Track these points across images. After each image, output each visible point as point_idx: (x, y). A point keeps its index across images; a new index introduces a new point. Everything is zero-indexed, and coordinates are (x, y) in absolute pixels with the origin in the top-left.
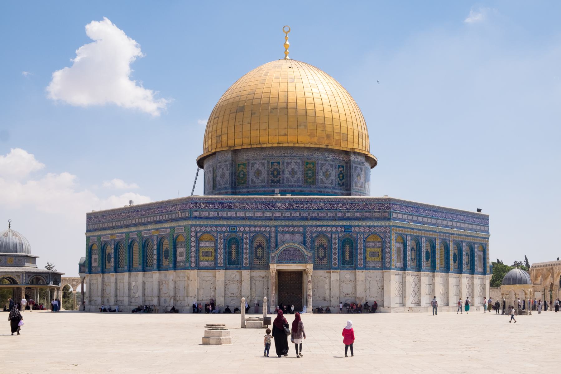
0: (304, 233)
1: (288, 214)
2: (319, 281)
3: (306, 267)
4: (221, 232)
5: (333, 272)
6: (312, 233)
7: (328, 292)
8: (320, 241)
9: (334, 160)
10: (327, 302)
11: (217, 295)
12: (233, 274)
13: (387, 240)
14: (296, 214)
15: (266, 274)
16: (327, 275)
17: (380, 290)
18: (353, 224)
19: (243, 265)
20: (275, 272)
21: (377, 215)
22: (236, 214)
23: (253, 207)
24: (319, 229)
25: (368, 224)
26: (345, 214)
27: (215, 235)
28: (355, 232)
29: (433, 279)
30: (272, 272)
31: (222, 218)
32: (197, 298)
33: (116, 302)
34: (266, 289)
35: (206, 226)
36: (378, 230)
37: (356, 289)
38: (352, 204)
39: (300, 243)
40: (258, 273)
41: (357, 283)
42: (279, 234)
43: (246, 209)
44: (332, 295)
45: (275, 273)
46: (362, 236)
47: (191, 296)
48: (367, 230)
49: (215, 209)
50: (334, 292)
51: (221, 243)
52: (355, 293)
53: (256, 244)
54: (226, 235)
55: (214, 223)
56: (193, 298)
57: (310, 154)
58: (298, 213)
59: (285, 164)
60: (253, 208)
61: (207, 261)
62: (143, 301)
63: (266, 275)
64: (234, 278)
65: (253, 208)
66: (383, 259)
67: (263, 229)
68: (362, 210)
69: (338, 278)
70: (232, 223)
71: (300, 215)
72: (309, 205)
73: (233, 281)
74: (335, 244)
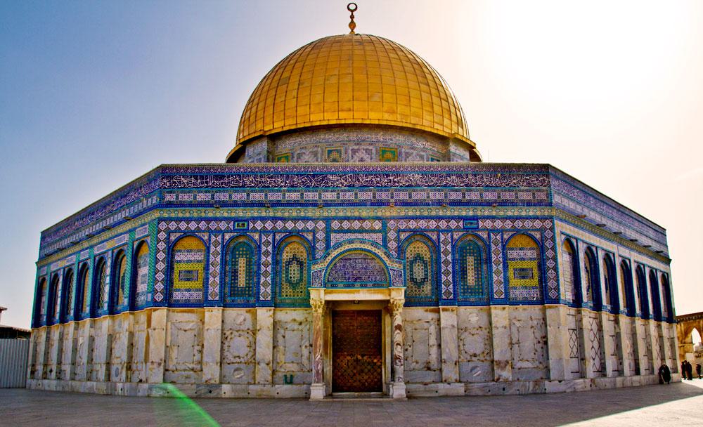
0: (384, 230)
1: (350, 196)
2: (416, 329)
3: (390, 295)
4: (218, 231)
5: (444, 310)
6: (399, 231)
7: (434, 350)
8: (415, 248)
9: (424, 150)
10: (433, 372)
11: (205, 359)
12: (237, 315)
13: (548, 244)
14: (368, 196)
15: (307, 316)
16: (431, 316)
17: (541, 345)
18: (479, 213)
19: (259, 297)
20: (322, 306)
21: (525, 196)
22: (248, 195)
23: (282, 182)
24: (412, 224)
25: (510, 214)
26: (464, 194)
27: (206, 238)
28: (486, 229)
29: (616, 326)
30: (315, 307)
31: (223, 204)
32: (165, 366)
33: (60, 373)
34: (306, 347)
35: (188, 220)
36: (528, 224)
37: (492, 345)
38: (475, 176)
39: (374, 244)
40: (286, 315)
41: (495, 331)
42: (333, 235)
43: (268, 187)
44: (444, 357)
45: (321, 309)
46: (499, 237)
47: (152, 362)
48: (508, 224)
49: (207, 187)
50: (447, 350)
51: (216, 253)
52: (491, 352)
53: (287, 256)
54: (227, 237)
55: (203, 215)
56: (155, 365)
57: (388, 137)
58: (371, 194)
59: (350, 152)
60: (282, 184)
61: (189, 290)
62: (87, 372)
63: (306, 318)
64: (241, 325)
65: (282, 184)
66: (542, 283)
67: (300, 225)
68: (496, 186)
69: (455, 324)
70: (240, 213)
71: (374, 197)
72: (391, 178)
73: (239, 330)
74: (446, 252)
